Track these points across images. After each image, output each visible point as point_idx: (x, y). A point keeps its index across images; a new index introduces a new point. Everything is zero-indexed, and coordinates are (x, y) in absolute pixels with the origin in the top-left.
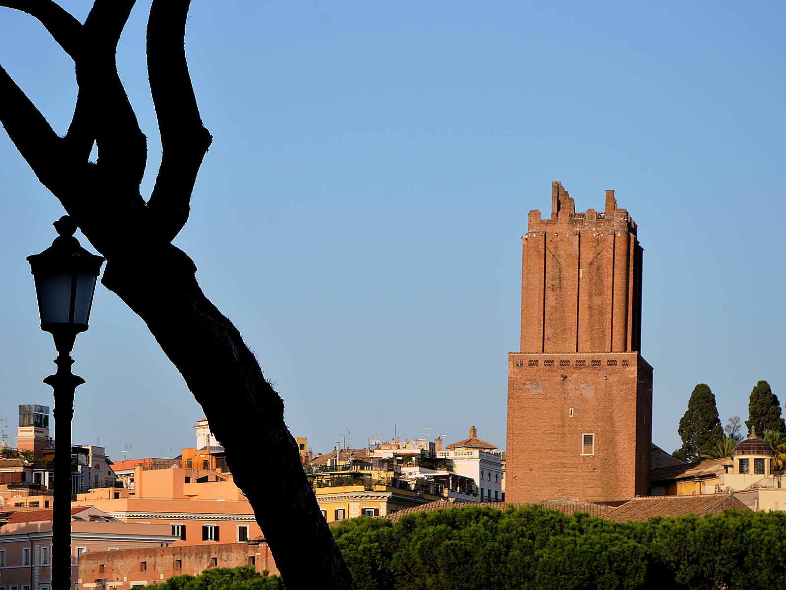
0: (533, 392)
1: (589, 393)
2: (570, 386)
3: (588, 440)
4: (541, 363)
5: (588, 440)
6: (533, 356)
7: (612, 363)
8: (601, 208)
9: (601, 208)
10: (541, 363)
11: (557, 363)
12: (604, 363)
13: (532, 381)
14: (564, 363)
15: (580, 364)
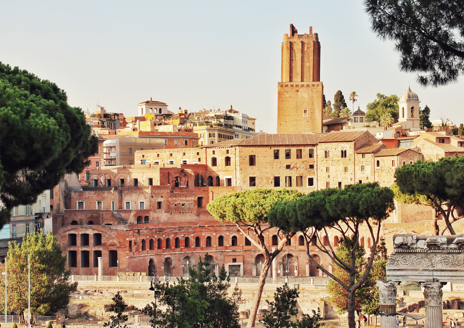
0: (287, 95)
1: (306, 96)
2: (299, 93)
3: (305, 111)
4: (289, 86)
5: (305, 111)
6: (287, 84)
7: (313, 85)
8: (308, 33)
9: (308, 33)
10: (289, 86)
11: (294, 86)
12: (311, 86)
13: (287, 92)
14: (297, 86)
15: (303, 86)
